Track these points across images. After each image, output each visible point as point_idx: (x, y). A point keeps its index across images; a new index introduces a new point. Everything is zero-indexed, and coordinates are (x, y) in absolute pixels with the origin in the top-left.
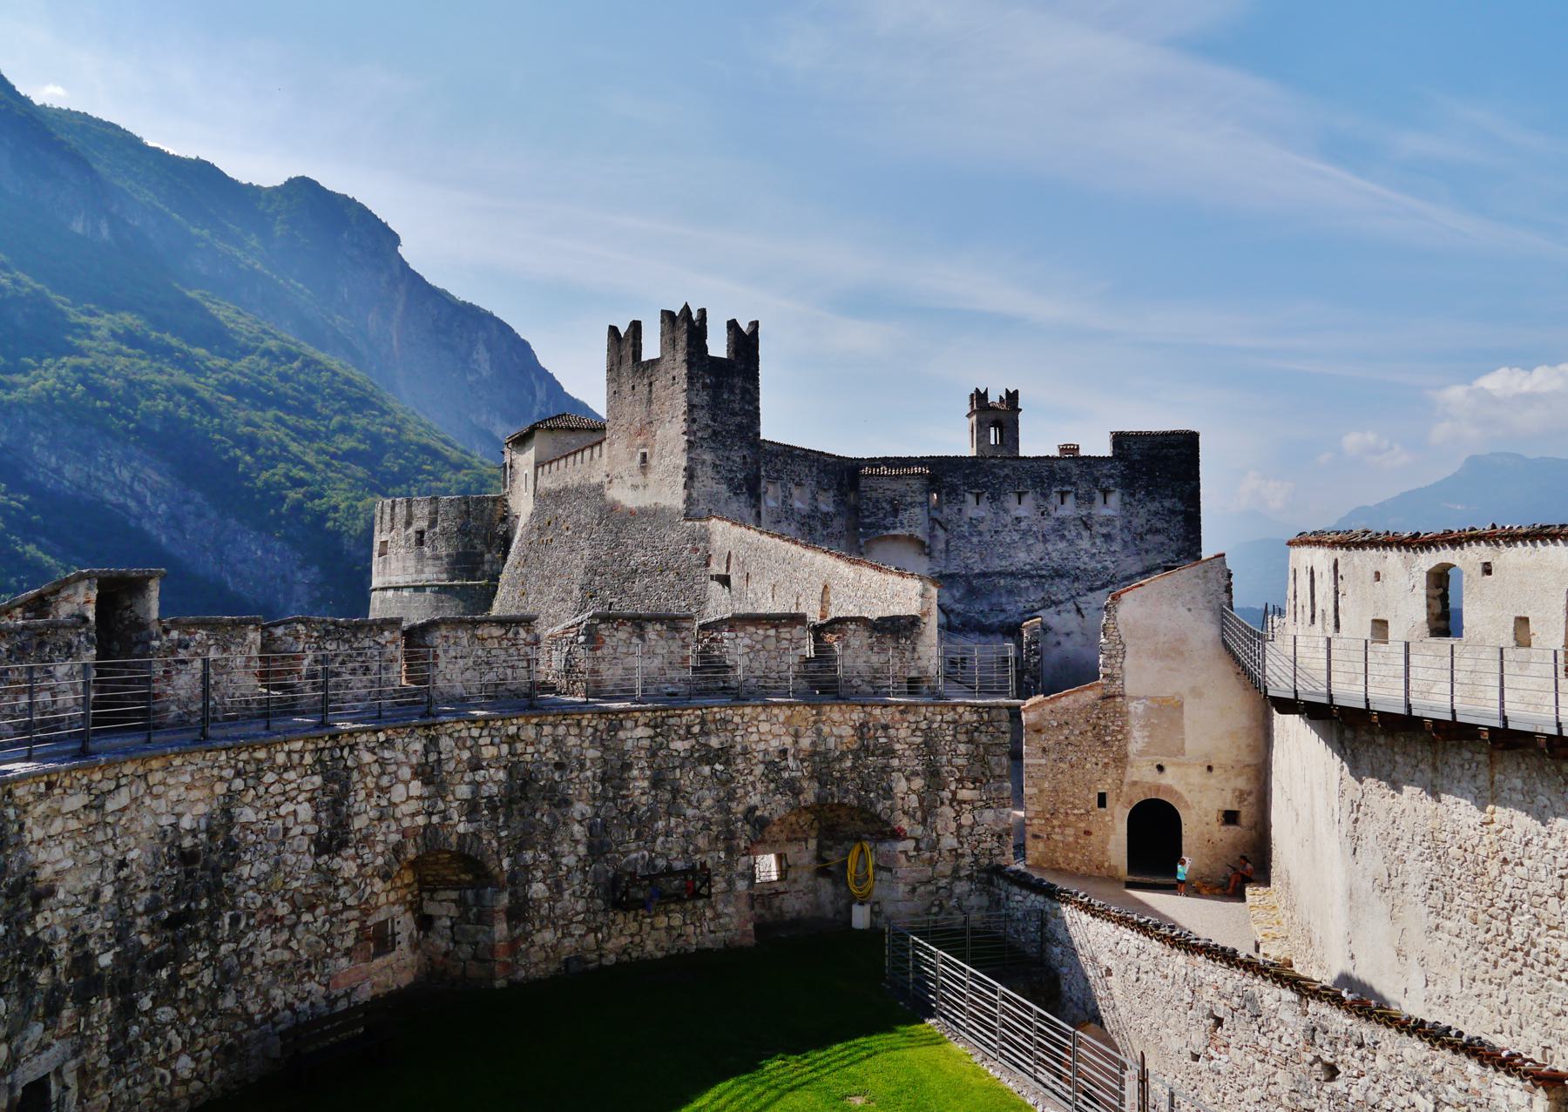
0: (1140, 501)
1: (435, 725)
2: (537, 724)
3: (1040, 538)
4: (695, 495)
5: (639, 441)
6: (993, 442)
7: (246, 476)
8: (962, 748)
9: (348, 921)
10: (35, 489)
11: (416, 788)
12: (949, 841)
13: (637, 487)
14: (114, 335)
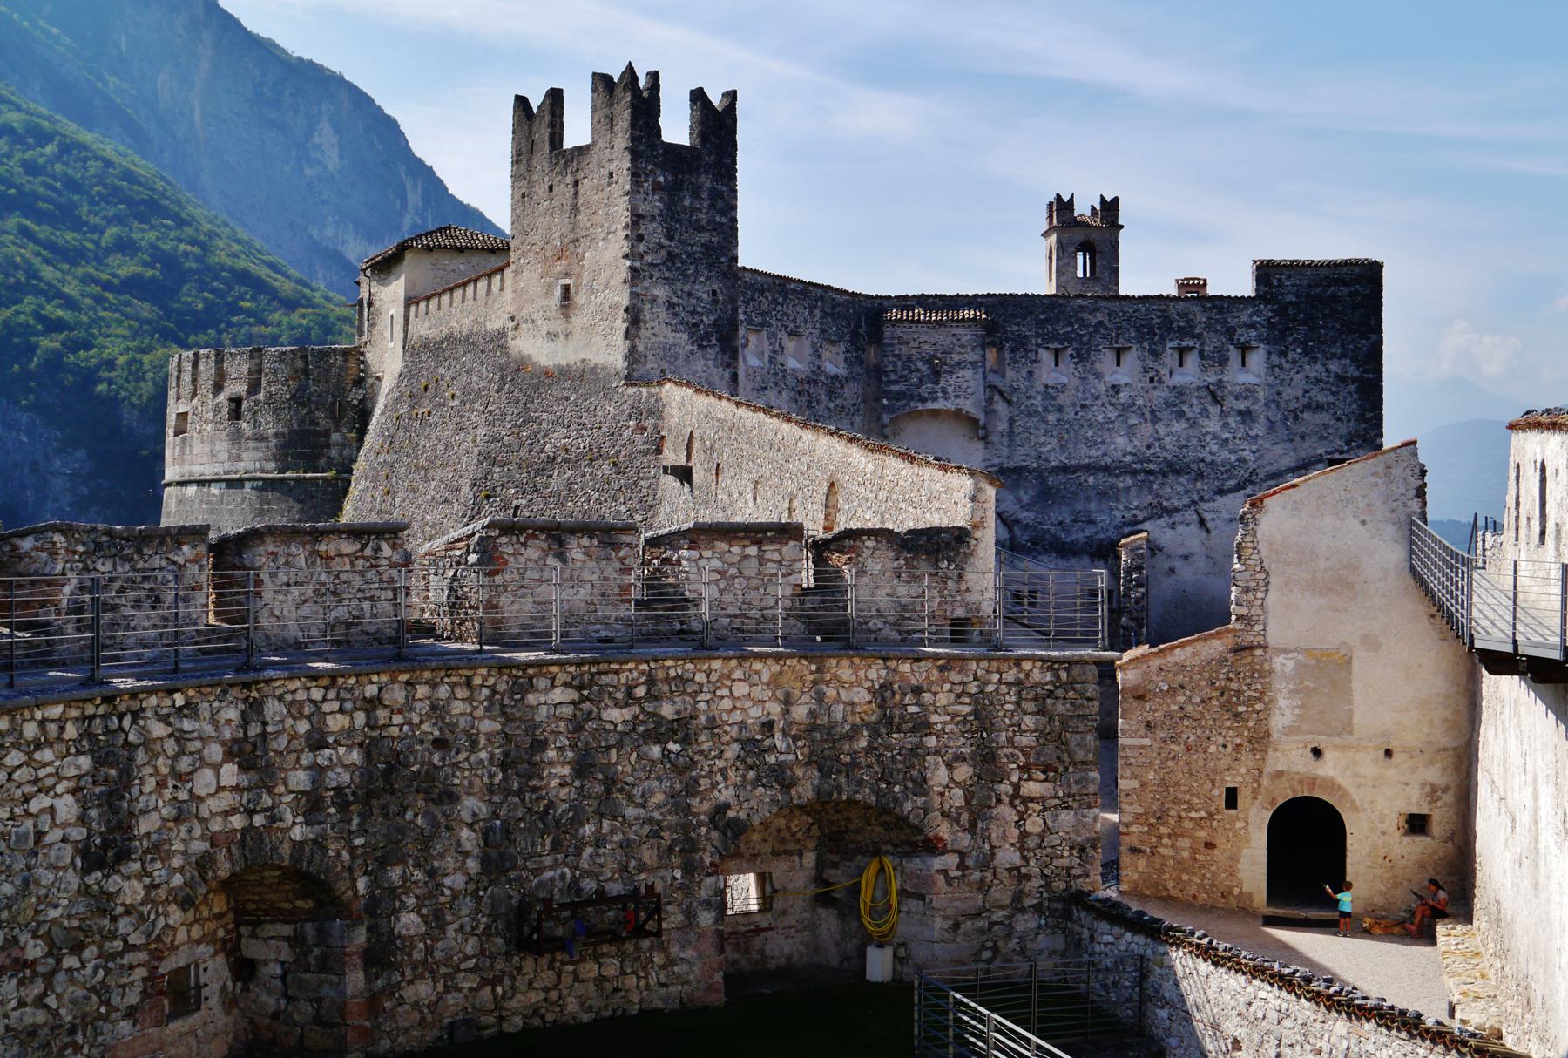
0: (1294, 362)
1: (257, 682)
2: (407, 683)
3: (1148, 415)
4: (641, 348)
5: (559, 267)
6: (1080, 274)
8: (1029, 722)
9: (132, 967)
11: (230, 774)
12: (1008, 856)
13: (556, 335)
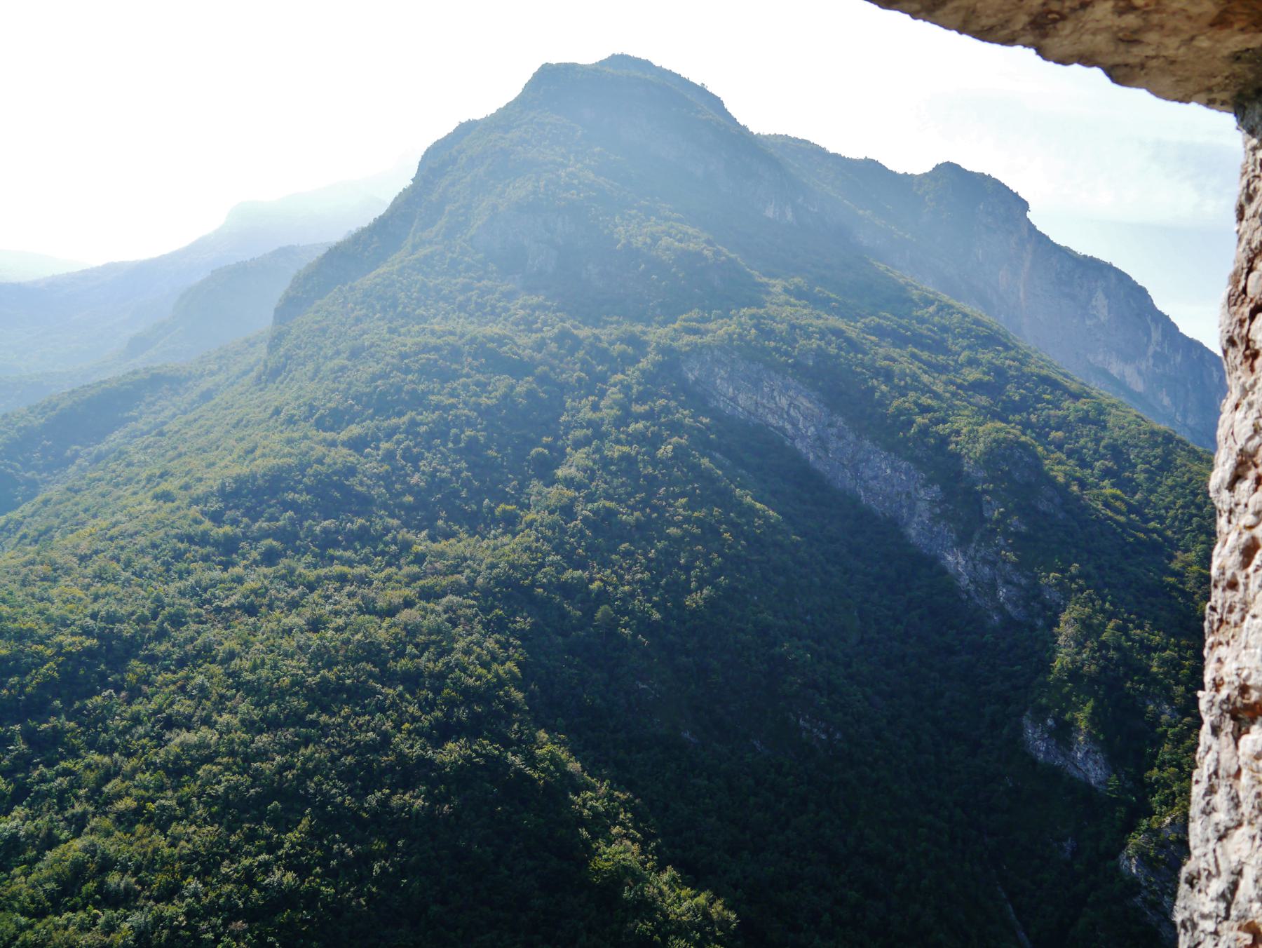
7: (881, 403)
10: (716, 414)
14: (786, 290)
